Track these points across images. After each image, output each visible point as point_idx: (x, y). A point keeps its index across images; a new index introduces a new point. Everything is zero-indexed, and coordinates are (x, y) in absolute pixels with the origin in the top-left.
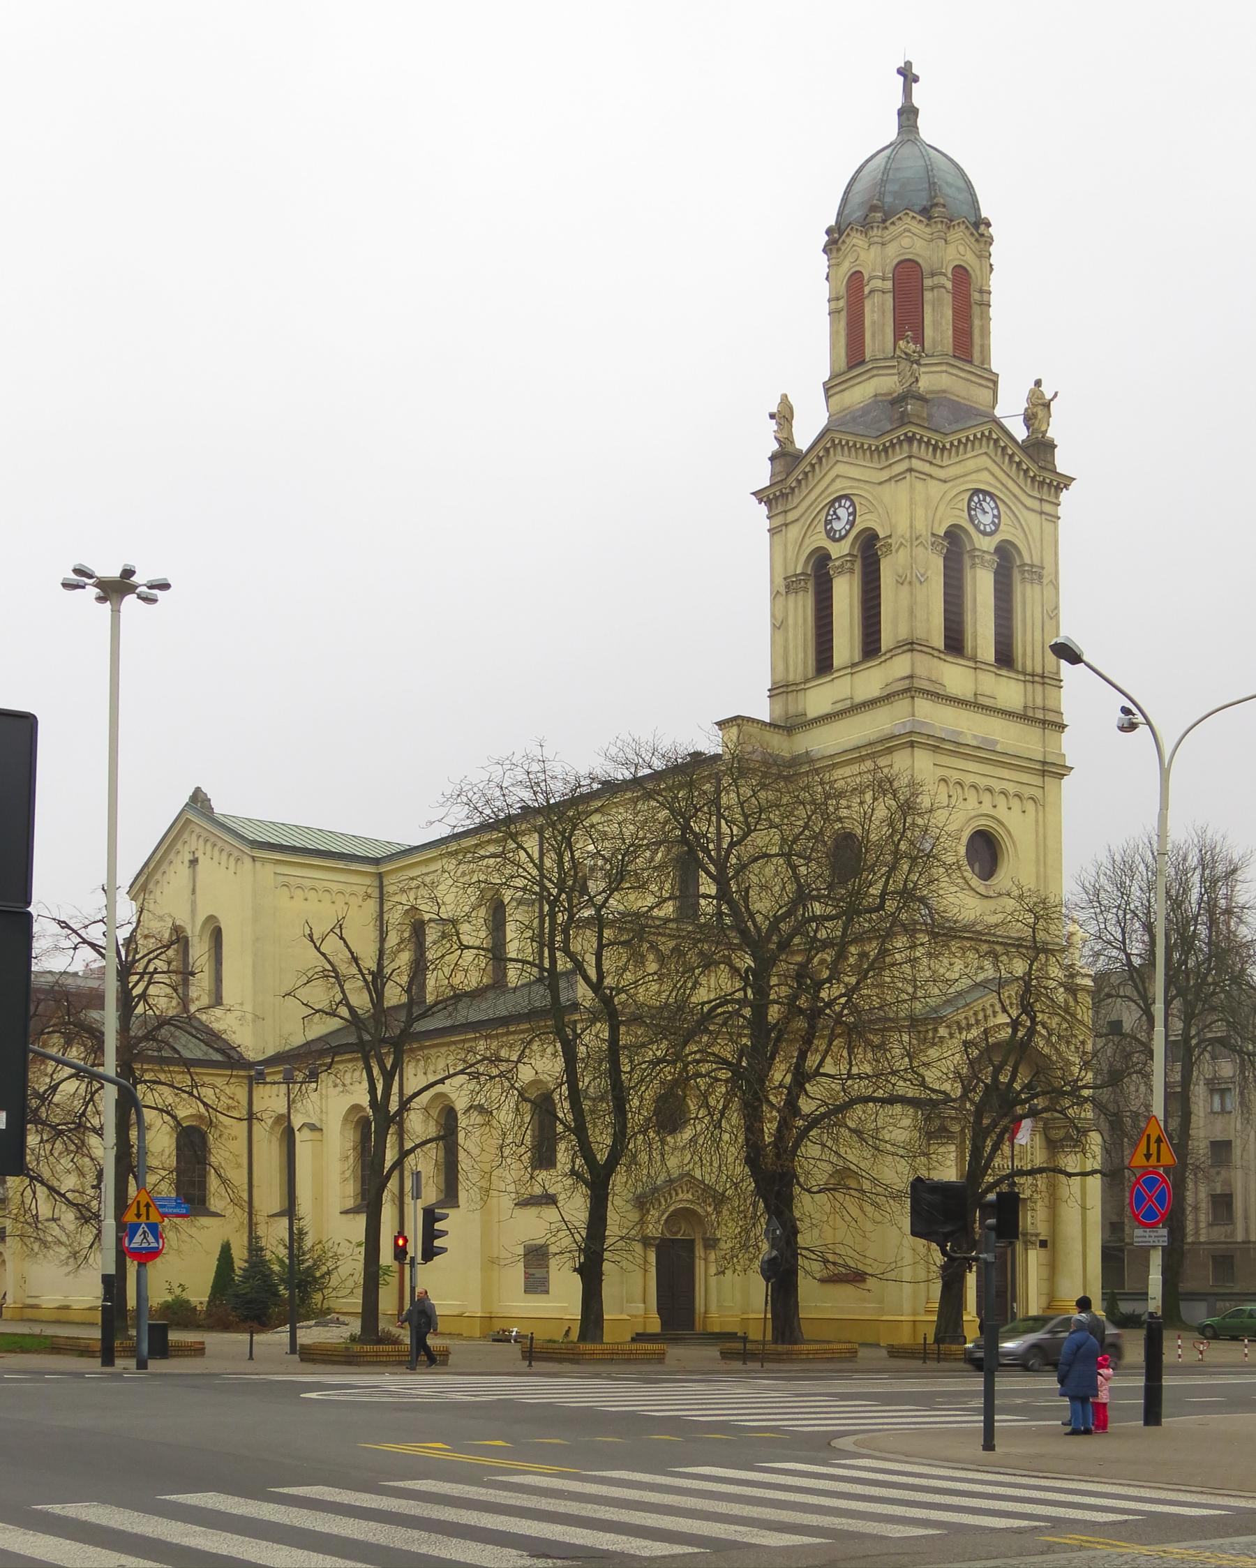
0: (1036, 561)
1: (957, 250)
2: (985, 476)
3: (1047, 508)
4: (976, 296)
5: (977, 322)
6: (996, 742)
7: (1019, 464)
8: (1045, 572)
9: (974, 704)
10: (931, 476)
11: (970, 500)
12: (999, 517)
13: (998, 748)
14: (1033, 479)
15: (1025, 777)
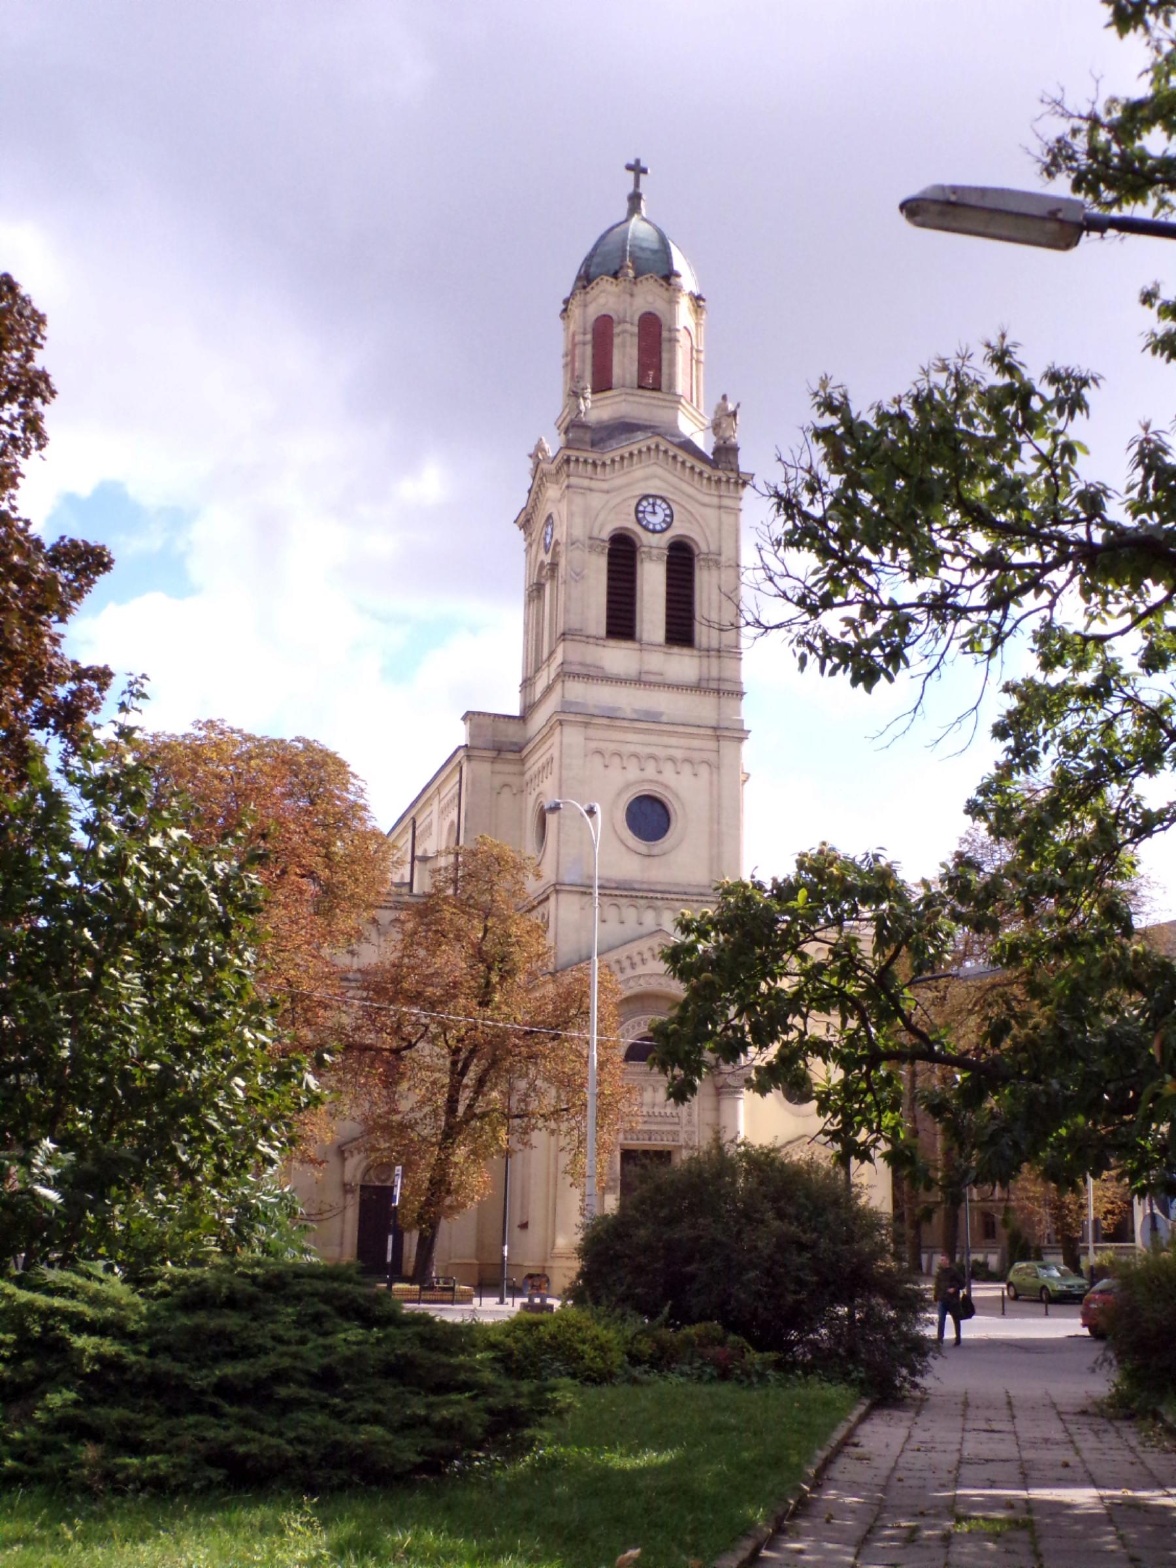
0: (713, 548)
1: (648, 297)
2: (658, 483)
3: (726, 502)
4: (665, 334)
5: (665, 355)
6: (661, 714)
7: (692, 468)
8: (723, 559)
9: (639, 681)
10: (591, 490)
11: (638, 504)
12: (671, 516)
13: (664, 719)
14: (709, 479)
15: (696, 743)
